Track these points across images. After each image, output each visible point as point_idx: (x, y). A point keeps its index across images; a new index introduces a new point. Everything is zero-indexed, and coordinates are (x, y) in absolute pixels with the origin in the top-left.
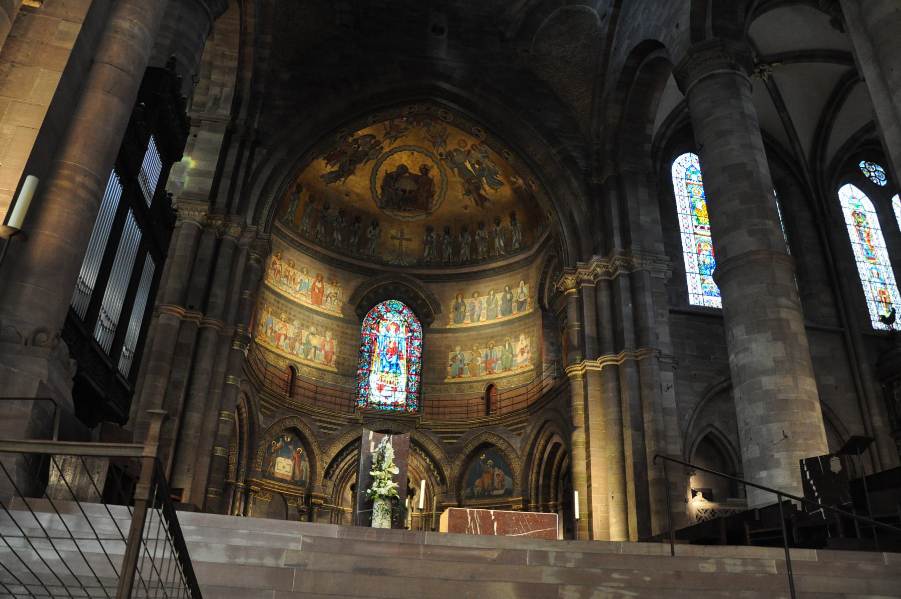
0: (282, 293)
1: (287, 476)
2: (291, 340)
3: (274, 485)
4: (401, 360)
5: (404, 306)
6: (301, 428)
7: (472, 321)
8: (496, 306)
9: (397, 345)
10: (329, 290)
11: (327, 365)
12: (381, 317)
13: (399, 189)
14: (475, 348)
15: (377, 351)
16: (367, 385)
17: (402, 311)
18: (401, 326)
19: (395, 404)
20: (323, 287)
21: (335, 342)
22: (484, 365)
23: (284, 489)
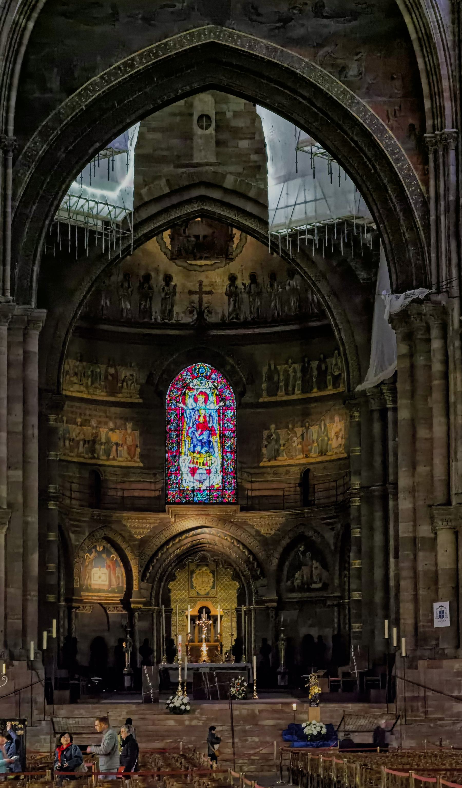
0: (74, 394)
1: (104, 585)
2: (91, 443)
3: (93, 596)
4: (214, 437)
5: (212, 369)
6: (111, 535)
7: (287, 394)
8: (311, 377)
9: (208, 419)
10: (124, 373)
11: (130, 461)
12: (187, 386)
13: (192, 236)
14: (290, 426)
15: (186, 428)
16: (178, 469)
17: (210, 376)
18: (210, 395)
19: (211, 489)
20: (116, 372)
21: (137, 433)
22: (300, 446)
23: (103, 598)
